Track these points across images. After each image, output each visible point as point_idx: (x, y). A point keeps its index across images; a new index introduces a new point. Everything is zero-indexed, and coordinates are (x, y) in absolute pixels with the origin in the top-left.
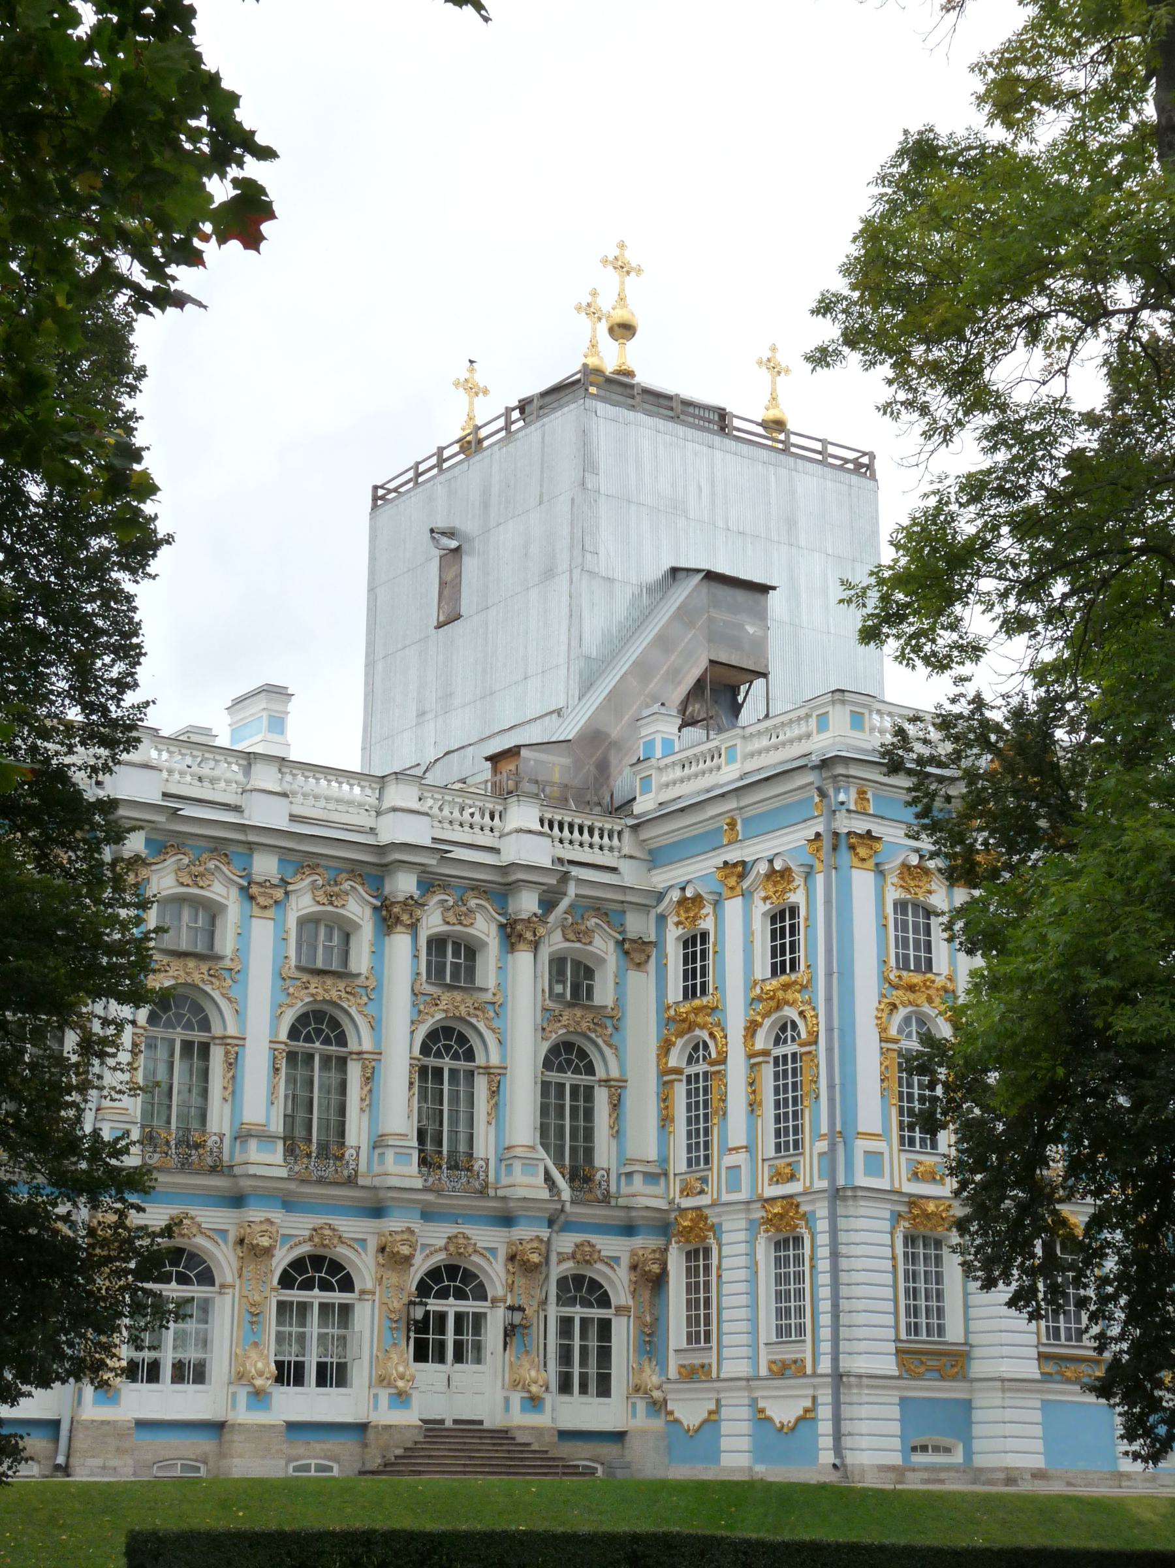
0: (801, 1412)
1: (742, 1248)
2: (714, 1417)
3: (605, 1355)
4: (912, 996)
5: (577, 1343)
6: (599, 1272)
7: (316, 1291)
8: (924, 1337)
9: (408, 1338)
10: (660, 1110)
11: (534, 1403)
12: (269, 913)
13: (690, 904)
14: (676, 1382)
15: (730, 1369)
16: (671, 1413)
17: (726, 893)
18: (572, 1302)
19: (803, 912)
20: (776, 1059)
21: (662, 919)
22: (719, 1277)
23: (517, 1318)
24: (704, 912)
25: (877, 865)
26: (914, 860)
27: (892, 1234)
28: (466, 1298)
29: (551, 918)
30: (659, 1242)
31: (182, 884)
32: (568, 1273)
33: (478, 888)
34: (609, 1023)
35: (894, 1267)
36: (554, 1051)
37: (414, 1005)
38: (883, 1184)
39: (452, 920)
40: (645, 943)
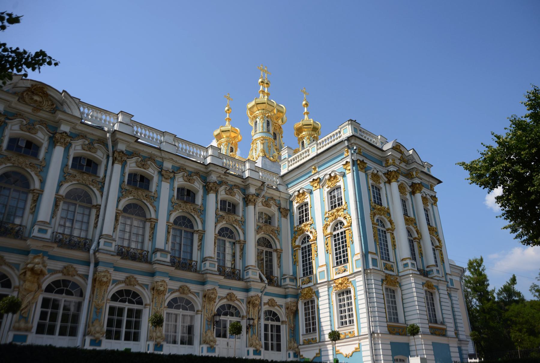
0: (354, 350)
2: (318, 355)
3: (279, 338)
9: (214, 328)
11: (257, 352)
12: (169, 181)
13: (301, 194)
14: (304, 344)
16: (302, 356)
17: (314, 189)
22: (318, 308)
24: (306, 197)
30: (296, 300)
31: (138, 167)
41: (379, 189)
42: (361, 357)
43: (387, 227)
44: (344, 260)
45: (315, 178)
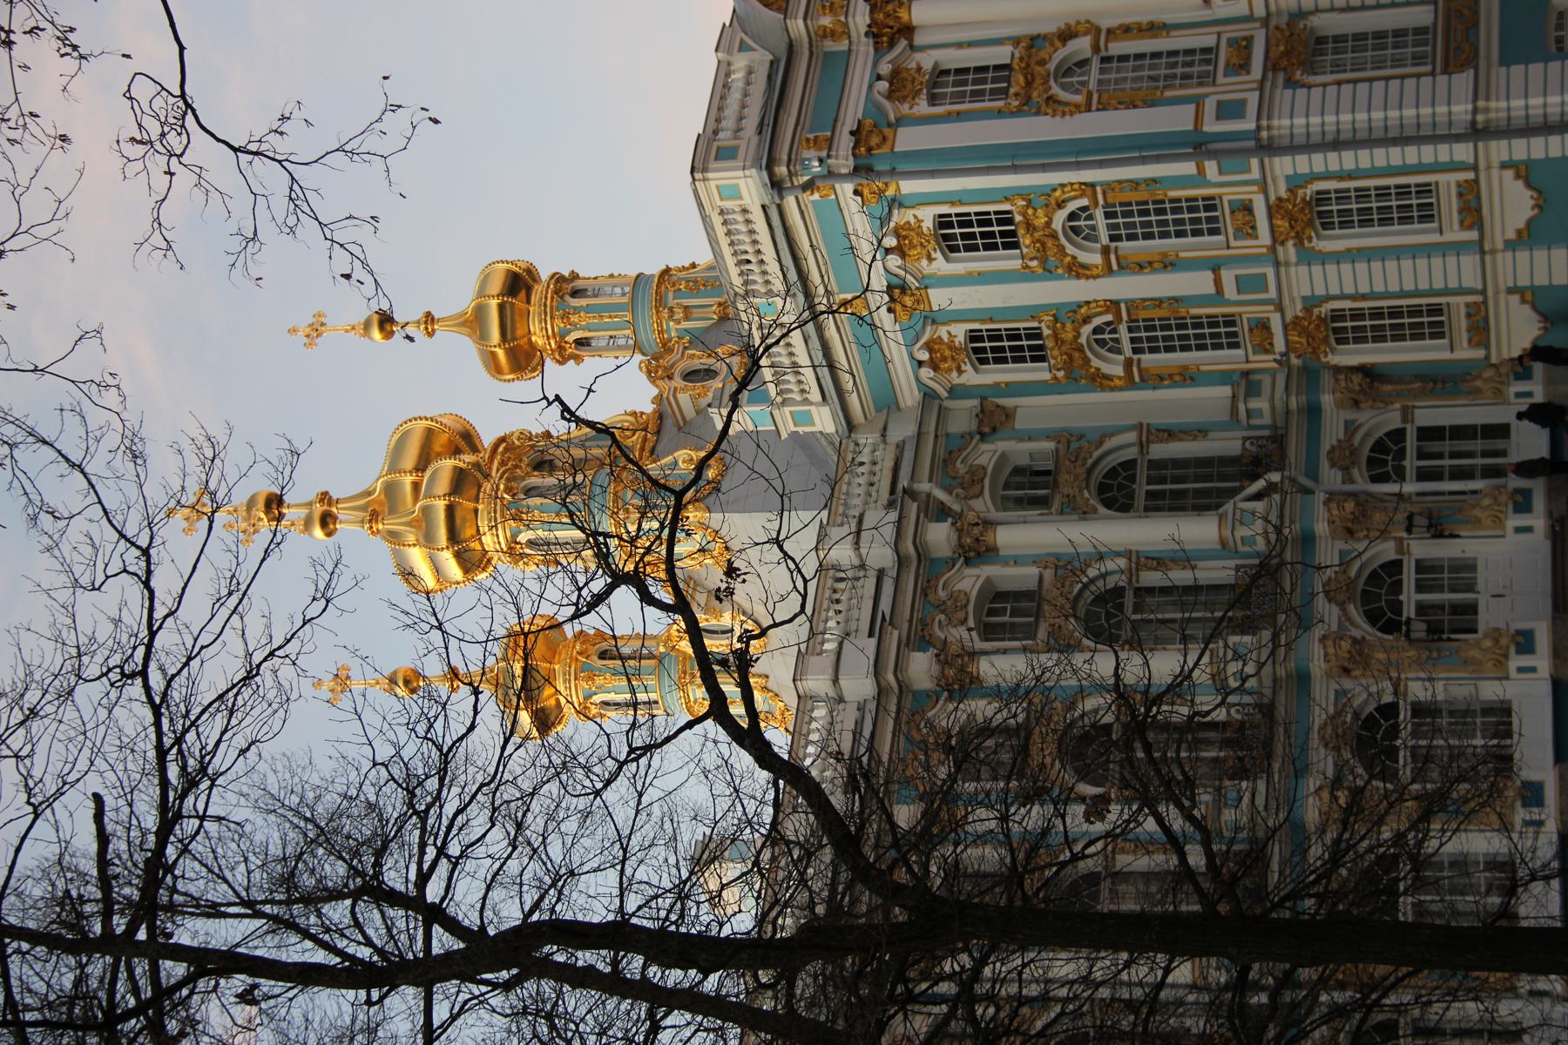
0: (1520, 184)
1: (1331, 269)
3: (1460, 432)
4: (1038, 81)
5: (1447, 462)
6: (1362, 441)
8: (1429, 48)
9: (1449, 640)
10: (1175, 385)
14: (1487, 347)
15: (1471, 279)
19: (945, 209)
20: (1113, 238)
21: (955, 392)
22: (1364, 297)
23: (1420, 521)
24: (945, 338)
25: (889, 125)
26: (883, 86)
27: (1309, 87)
28: (1400, 582)
29: (956, 507)
30: (1327, 379)
32: (1366, 474)
33: (925, 589)
34: (1074, 446)
35: (1348, 82)
36: (1108, 504)
38: (1253, 99)
40: (982, 411)
41: (941, 73)
42: (1548, 160)
43: (1088, 53)
44: (1207, 208)
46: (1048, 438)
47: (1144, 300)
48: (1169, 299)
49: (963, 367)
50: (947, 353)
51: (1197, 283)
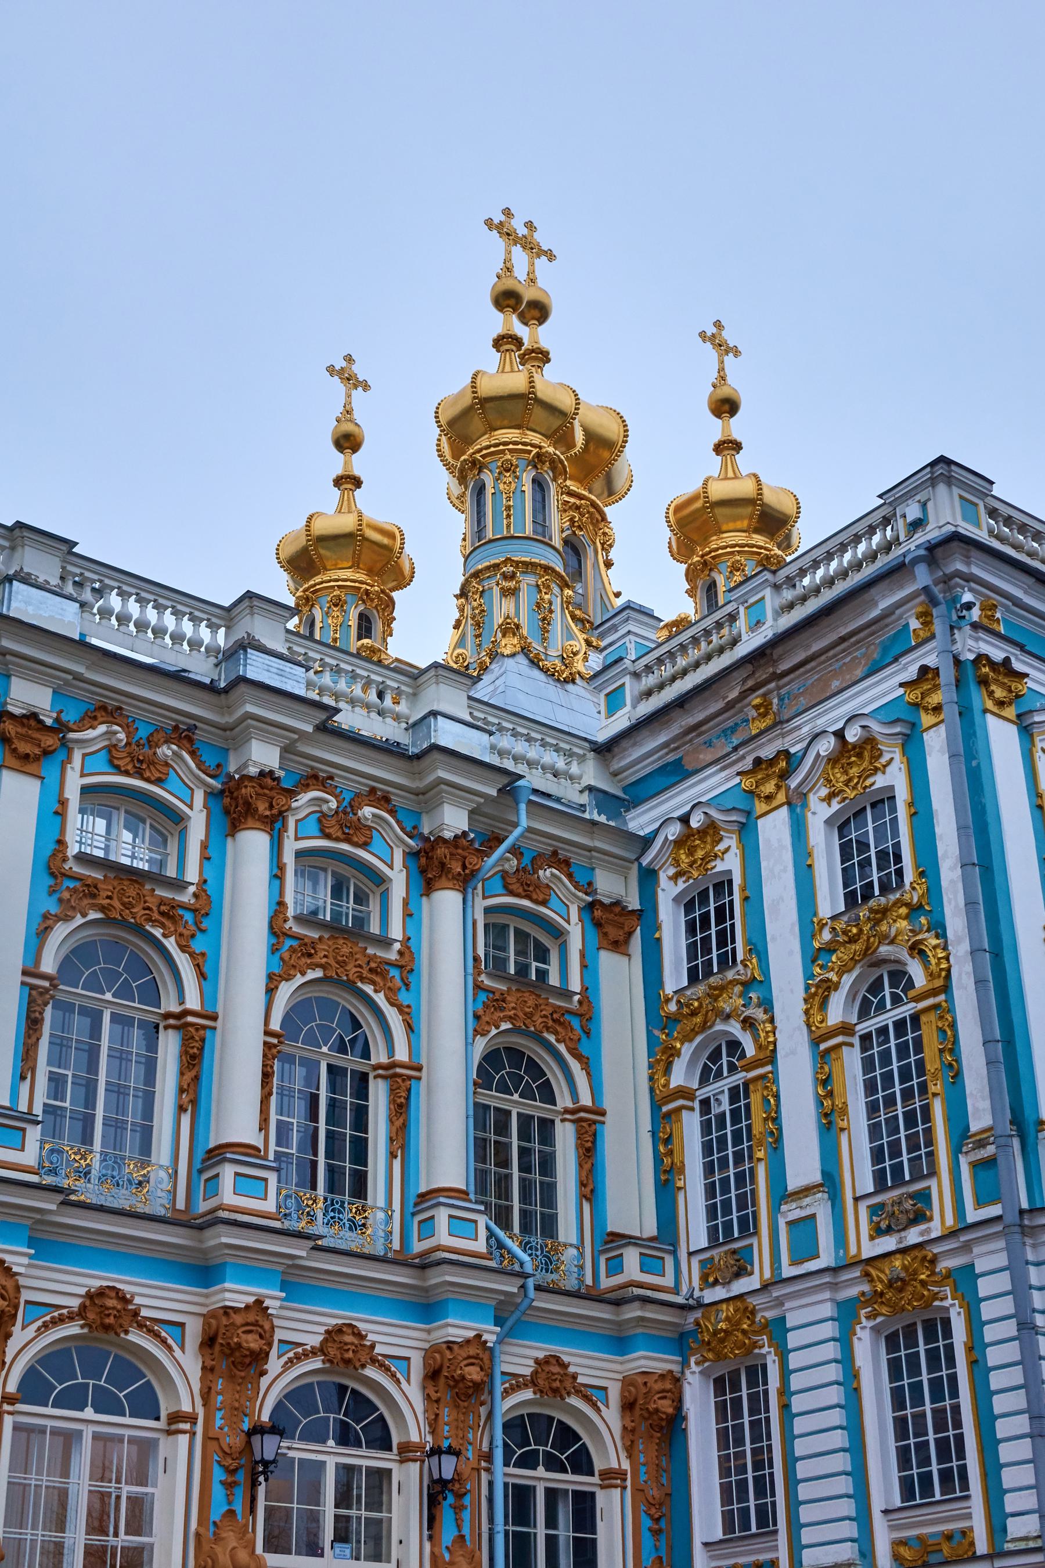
5: (541, 1531)
7: (89, 1413)
10: (658, 1159)
13: (696, 839)
17: (760, 807)
18: (528, 1461)
20: (866, 1038)
21: (648, 877)
22: (785, 1407)
24: (721, 847)
36: (491, 1058)
37: (274, 949)
39: (334, 831)
45: (767, 752)
46: (585, 989)
47: (777, 1097)
48: (780, 1130)
49: (680, 881)
50: (700, 854)
51: (802, 1164)
